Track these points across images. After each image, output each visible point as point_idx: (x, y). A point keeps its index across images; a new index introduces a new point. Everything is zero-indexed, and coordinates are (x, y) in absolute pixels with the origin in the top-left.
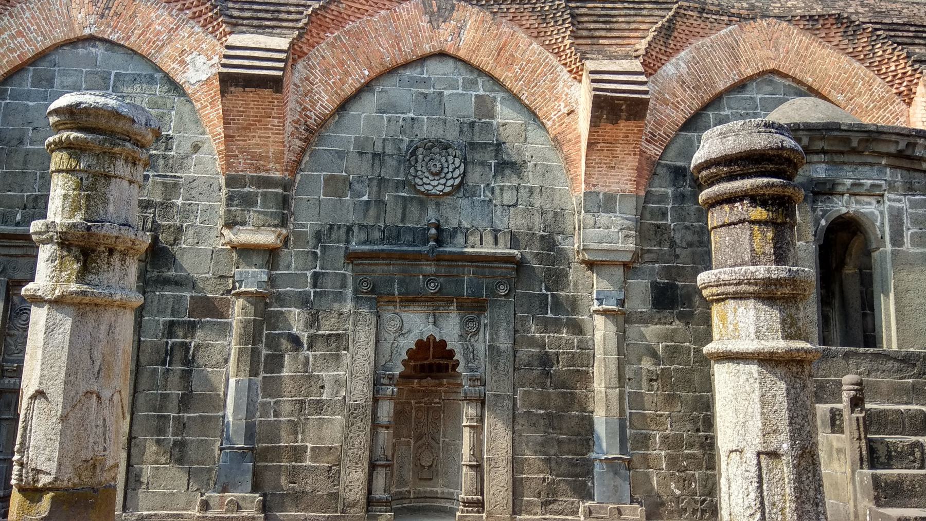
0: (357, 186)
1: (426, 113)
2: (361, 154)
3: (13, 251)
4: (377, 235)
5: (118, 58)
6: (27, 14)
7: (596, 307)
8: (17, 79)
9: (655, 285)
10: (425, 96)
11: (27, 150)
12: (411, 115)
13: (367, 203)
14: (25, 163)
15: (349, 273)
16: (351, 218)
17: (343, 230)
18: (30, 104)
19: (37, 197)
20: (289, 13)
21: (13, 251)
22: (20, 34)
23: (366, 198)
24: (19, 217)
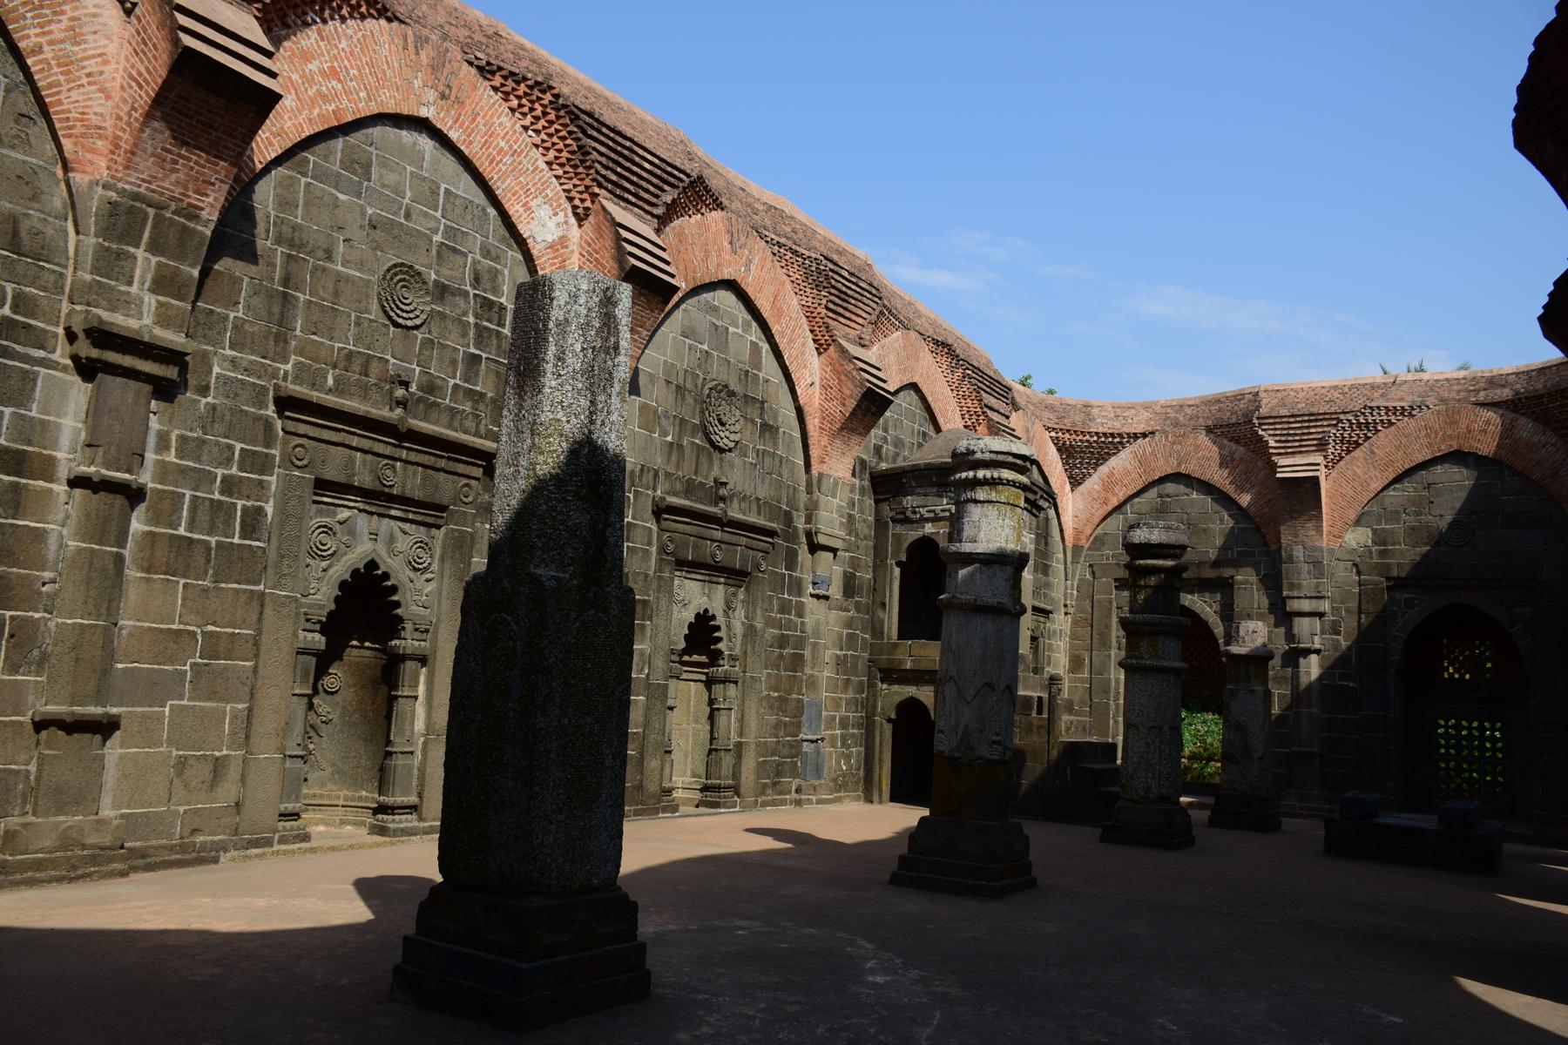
0: (664, 422)
1: (716, 349)
2: (668, 382)
3: (326, 435)
4: (678, 486)
5: (450, 164)
6: (344, 44)
7: (810, 590)
8: (321, 148)
9: (845, 572)
10: (716, 327)
11: (338, 272)
12: (705, 347)
13: (671, 444)
14: (336, 293)
15: (655, 528)
16: (658, 461)
17: (652, 474)
18: (342, 197)
19: (351, 352)
20: (647, 191)
21: (326, 435)
22: (334, 73)
23: (669, 438)
24: (330, 381)
